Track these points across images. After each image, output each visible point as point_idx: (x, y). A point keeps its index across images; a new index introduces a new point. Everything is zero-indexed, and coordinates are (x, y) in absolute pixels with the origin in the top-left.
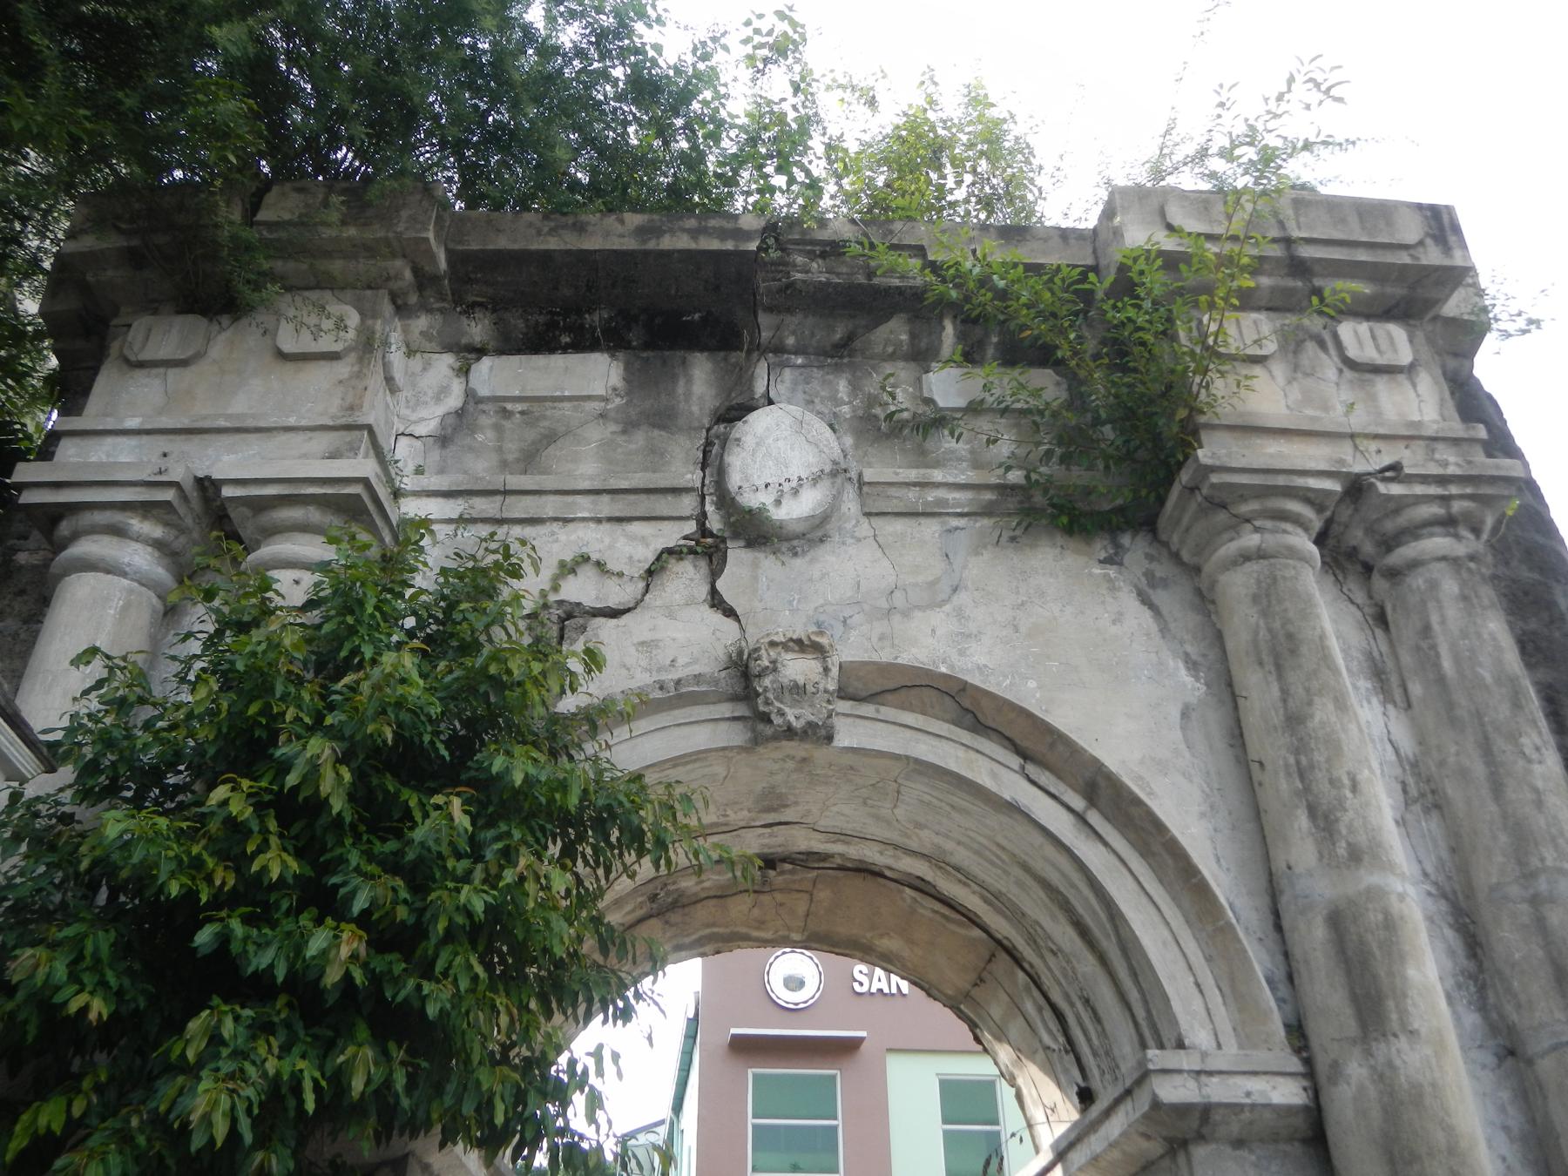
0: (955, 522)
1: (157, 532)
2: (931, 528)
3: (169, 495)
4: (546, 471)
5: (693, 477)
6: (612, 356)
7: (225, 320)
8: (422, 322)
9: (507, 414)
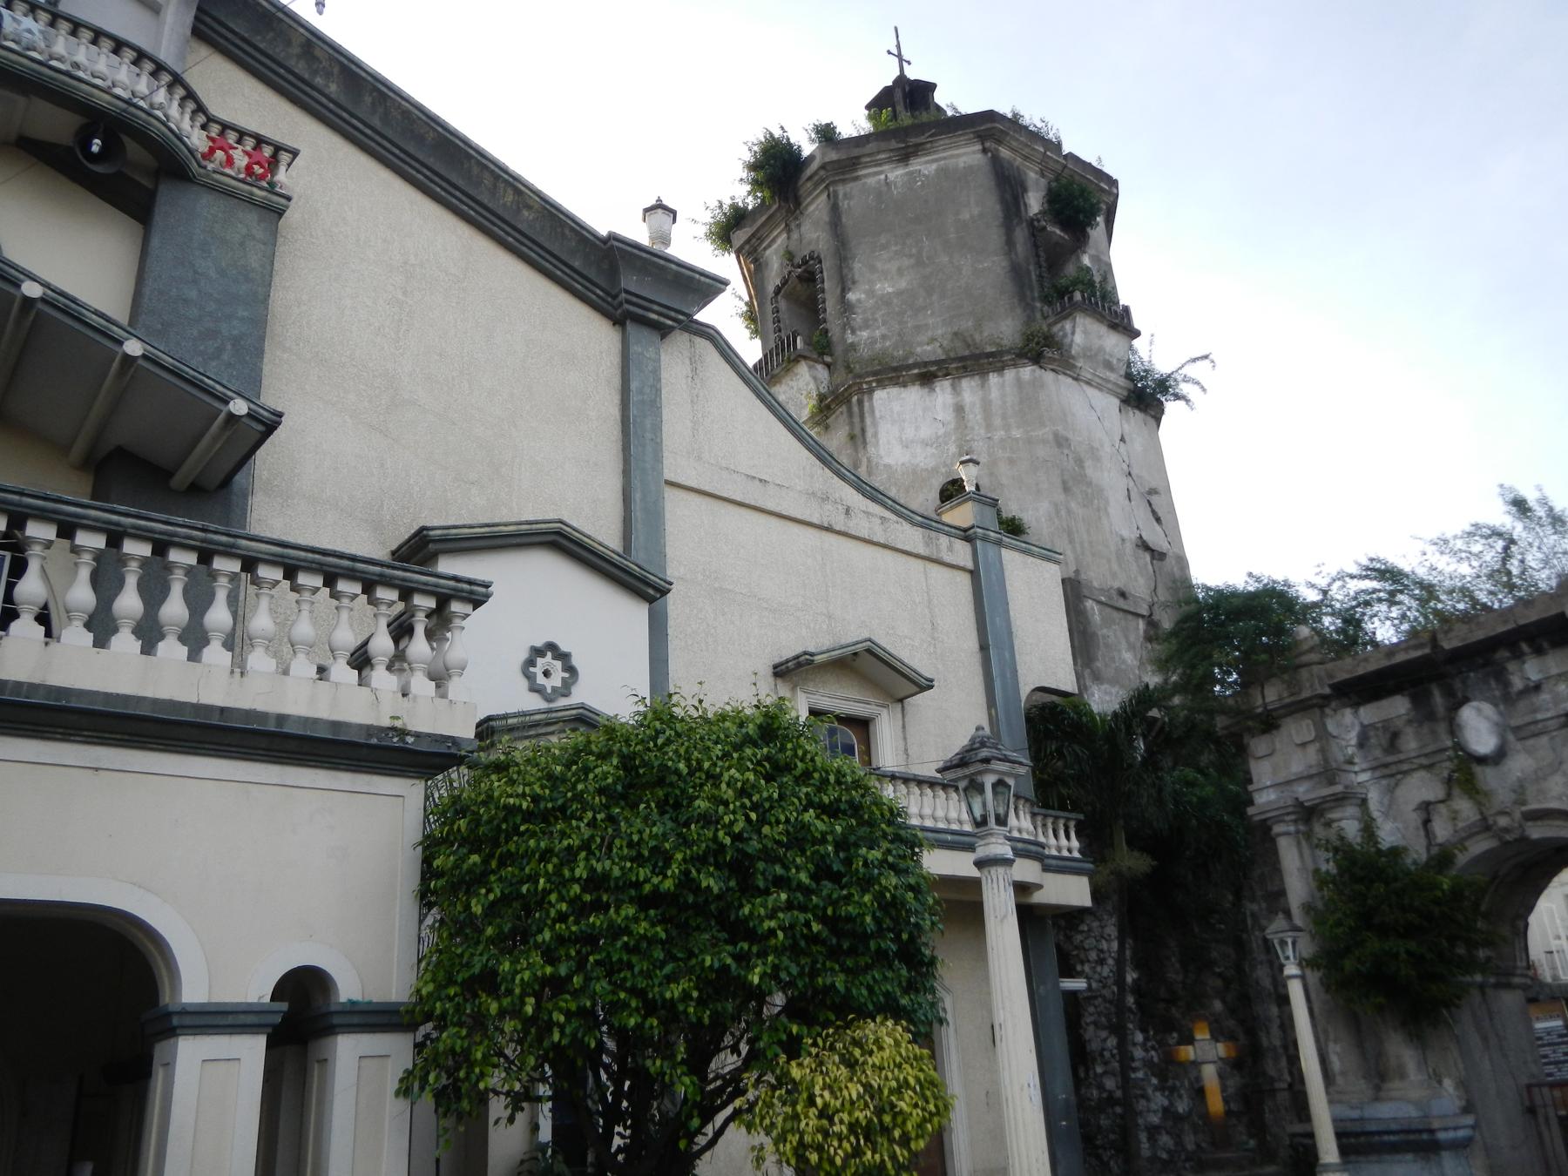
0: (1555, 733)
1: (1293, 817)
2: (1544, 740)
3: (1290, 810)
4: (1400, 752)
5: (1449, 743)
6: (1403, 695)
7: (1274, 732)
8: (1333, 704)
9: (1377, 729)
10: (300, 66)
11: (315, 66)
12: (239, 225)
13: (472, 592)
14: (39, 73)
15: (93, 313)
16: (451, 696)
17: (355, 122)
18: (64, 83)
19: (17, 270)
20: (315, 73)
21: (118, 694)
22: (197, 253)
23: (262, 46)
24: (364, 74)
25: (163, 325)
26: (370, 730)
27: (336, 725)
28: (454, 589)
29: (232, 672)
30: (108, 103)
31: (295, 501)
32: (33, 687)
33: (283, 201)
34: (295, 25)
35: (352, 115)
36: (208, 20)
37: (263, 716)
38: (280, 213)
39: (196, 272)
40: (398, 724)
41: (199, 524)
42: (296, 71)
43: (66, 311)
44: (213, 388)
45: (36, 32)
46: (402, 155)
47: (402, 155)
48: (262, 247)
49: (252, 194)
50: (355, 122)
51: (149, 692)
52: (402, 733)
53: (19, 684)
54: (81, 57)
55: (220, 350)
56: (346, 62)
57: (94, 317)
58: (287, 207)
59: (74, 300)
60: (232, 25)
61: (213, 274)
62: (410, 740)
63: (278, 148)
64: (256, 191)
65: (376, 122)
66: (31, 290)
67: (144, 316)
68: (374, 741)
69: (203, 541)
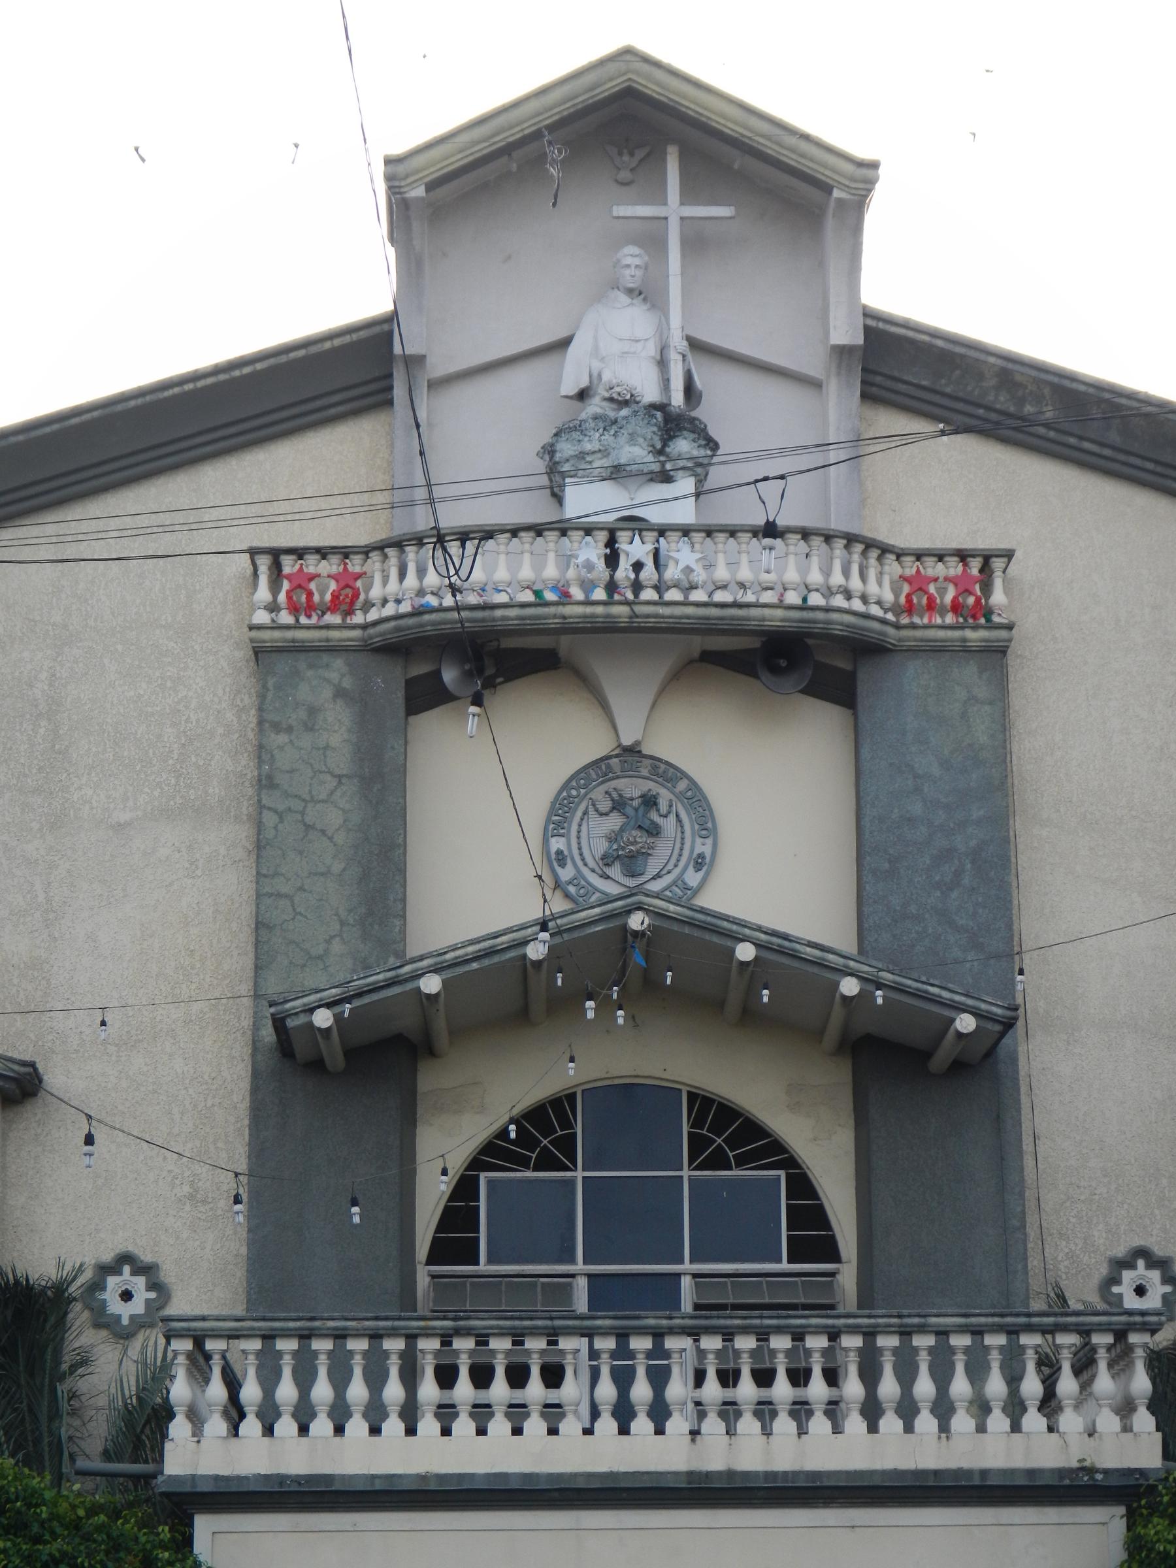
10: (1002, 399)
11: (1020, 393)
12: (957, 688)
13: (1144, 1323)
14: (708, 618)
15: (805, 945)
16: (1135, 1429)
17: (1086, 445)
18: (732, 618)
19: (728, 921)
20: (1021, 402)
21: (855, 1471)
22: (913, 749)
23: (948, 390)
24: (1082, 388)
25: (890, 862)
26: (1061, 1472)
27: (1031, 1473)
28: (1128, 1324)
29: (939, 1438)
30: (782, 620)
31: (1082, 1032)
32: (796, 1474)
33: (1003, 634)
34: (982, 357)
35: (1081, 438)
36: (878, 379)
37: (968, 1473)
38: (1002, 651)
39: (916, 776)
40: (1087, 1464)
41: (894, 1312)
42: (998, 406)
43: (781, 952)
44: (940, 997)
45: (694, 566)
46: (1159, 469)
47: (1159, 469)
48: (987, 708)
49: (964, 640)
50: (1086, 445)
51: (878, 1466)
52: (1091, 1471)
53: (785, 1473)
54: (745, 574)
55: (958, 874)
56: (1056, 380)
57: (808, 950)
58: (1010, 640)
59: (785, 937)
60: (905, 378)
61: (936, 771)
62: (1099, 1477)
63: (987, 558)
64: (969, 634)
65: (1114, 437)
66: (745, 952)
67: (868, 858)
68: (1067, 1482)
69: (901, 1326)
